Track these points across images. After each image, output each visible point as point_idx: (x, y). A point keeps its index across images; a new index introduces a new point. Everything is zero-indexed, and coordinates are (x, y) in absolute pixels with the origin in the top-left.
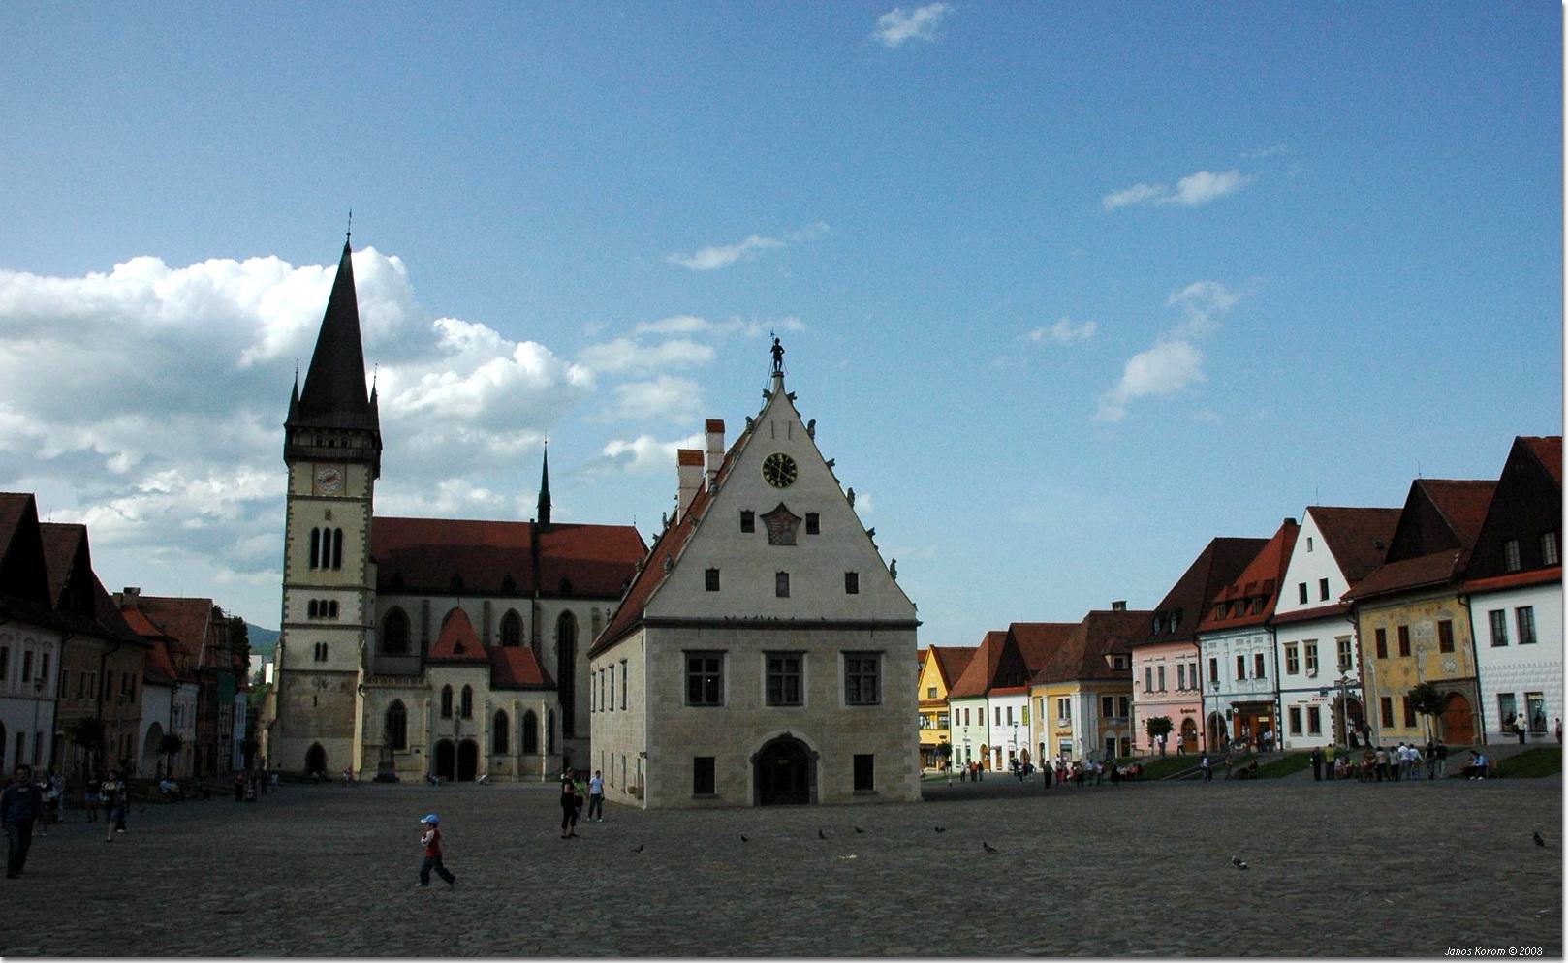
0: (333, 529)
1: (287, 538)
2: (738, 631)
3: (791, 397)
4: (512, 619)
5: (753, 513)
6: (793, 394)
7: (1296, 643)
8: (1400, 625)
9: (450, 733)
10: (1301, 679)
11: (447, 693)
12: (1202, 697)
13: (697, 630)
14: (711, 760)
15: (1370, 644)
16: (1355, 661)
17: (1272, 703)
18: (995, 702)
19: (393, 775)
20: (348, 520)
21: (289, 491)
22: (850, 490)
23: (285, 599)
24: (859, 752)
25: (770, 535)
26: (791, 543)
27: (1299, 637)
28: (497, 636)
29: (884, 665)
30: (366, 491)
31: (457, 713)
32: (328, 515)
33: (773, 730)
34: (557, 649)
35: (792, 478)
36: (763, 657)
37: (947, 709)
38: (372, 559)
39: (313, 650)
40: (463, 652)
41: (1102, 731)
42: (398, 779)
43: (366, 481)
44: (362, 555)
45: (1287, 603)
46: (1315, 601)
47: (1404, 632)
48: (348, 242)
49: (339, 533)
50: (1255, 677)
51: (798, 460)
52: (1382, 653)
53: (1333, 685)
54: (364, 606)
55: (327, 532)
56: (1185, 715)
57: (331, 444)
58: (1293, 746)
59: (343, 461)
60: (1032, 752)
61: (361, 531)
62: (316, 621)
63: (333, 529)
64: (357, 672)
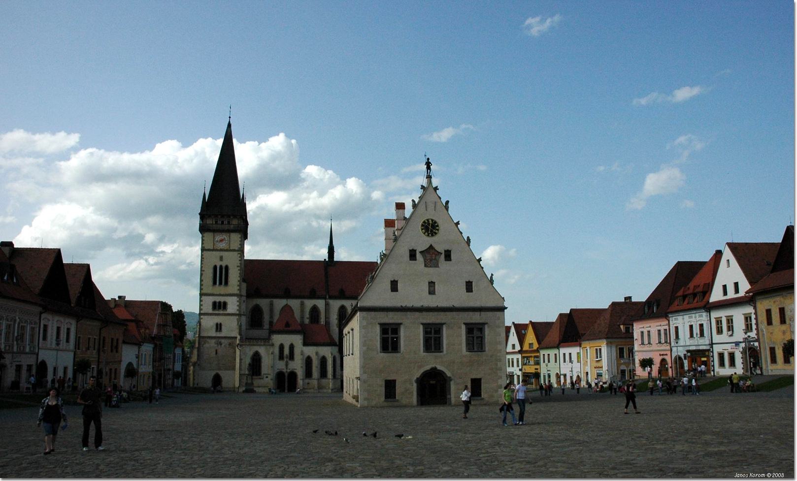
0: (224, 266)
1: (201, 270)
2: (408, 313)
3: (436, 189)
4: (315, 310)
5: (415, 251)
6: (437, 187)
7: (721, 317)
8: (780, 307)
9: (283, 368)
10: (724, 337)
11: (282, 347)
12: (670, 347)
13: (386, 313)
14: (394, 381)
15: (763, 317)
16: (754, 327)
17: (708, 350)
18: (563, 350)
19: (253, 389)
20: (231, 261)
21: (202, 247)
22: (468, 237)
23: (201, 301)
24: (474, 377)
25: (425, 262)
26: (437, 266)
27: (723, 314)
28: (307, 318)
29: (487, 331)
30: (240, 246)
31: (287, 358)
32: (221, 258)
33: (427, 365)
34: (338, 325)
35: (436, 231)
36: (421, 327)
37: (538, 354)
38: (244, 280)
39: (215, 327)
40: (289, 327)
41: (618, 365)
42: (255, 391)
43: (240, 241)
44: (239, 279)
45: (716, 295)
46: (731, 295)
48: (229, 122)
49: (227, 267)
50: (699, 336)
51: (440, 222)
52: (770, 322)
53: (742, 341)
54: (240, 303)
55: (221, 267)
56: (662, 357)
57: (223, 223)
58: (720, 374)
59: (229, 231)
60: (582, 376)
61: (238, 266)
62: (217, 312)
63: (224, 266)
64: (236, 338)
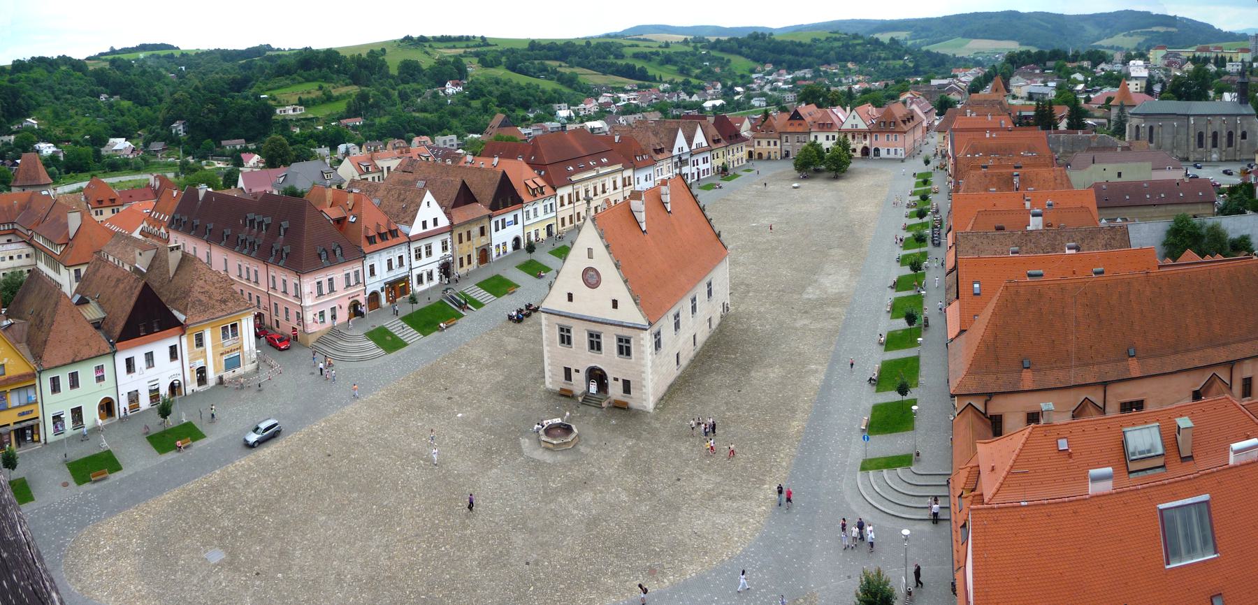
15: (456, 239)
16: (449, 247)
27: (422, 245)
46: (430, 227)
47: (469, 233)
52: (461, 241)
56: (351, 300)
